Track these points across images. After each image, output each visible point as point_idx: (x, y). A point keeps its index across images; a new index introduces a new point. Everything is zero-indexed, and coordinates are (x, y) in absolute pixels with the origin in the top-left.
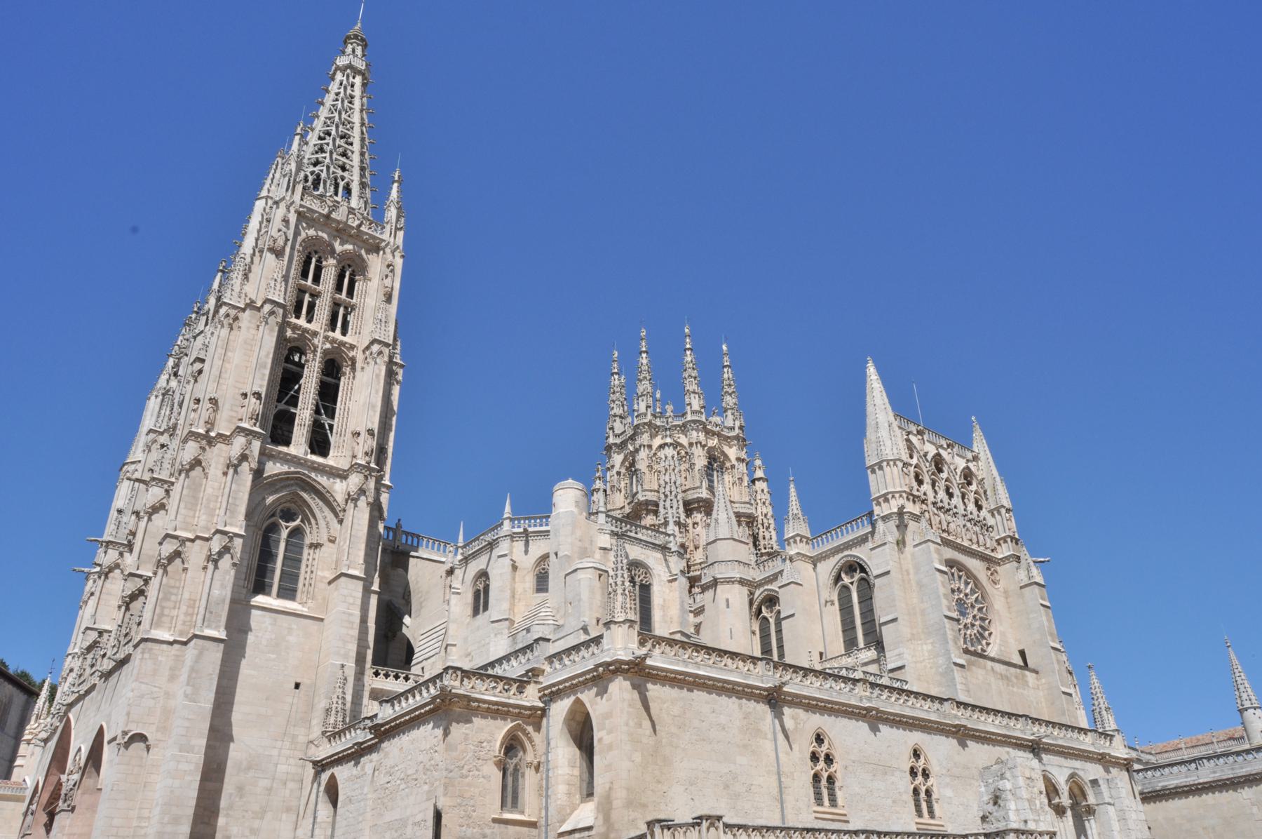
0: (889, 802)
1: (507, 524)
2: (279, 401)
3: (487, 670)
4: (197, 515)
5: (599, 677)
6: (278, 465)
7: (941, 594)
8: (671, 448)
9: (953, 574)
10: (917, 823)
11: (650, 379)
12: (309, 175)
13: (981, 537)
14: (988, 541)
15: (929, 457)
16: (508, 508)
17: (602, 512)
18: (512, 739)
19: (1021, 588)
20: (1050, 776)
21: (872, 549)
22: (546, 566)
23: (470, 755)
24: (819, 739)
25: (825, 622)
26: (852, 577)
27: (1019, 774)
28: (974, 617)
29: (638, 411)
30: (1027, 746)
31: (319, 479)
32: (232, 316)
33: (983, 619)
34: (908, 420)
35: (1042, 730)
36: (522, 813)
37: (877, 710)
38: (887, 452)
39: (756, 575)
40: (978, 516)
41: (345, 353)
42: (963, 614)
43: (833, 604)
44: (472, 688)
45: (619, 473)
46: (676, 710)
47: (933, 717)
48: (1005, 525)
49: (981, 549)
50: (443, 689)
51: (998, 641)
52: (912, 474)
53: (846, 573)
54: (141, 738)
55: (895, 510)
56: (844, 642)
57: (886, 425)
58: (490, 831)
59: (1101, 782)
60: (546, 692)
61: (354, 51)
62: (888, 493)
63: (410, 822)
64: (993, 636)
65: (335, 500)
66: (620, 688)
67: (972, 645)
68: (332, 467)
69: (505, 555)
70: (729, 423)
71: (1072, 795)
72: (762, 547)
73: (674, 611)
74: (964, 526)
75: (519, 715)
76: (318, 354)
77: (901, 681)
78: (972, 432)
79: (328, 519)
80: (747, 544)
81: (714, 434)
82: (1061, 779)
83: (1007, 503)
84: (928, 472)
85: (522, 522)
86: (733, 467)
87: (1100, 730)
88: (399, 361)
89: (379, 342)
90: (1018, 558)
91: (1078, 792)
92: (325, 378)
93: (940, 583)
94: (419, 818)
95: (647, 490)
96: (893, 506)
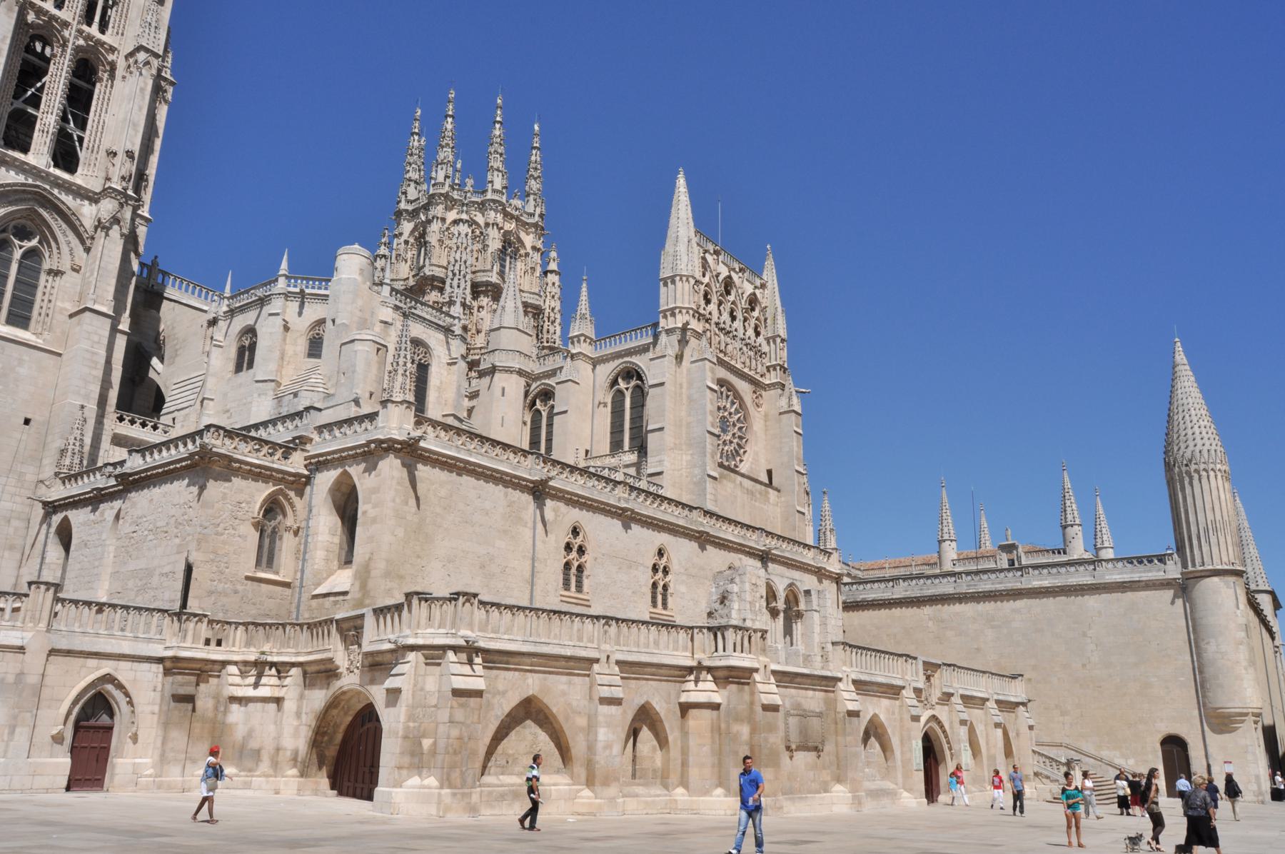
0: (629, 592)
1: (281, 284)
2: (16, 97)
3: (250, 431)
5: (370, 453)
6: (12, 173)
7: (708, 410)
8: (466, 225)
9: (722, 393)
10: (651, 613)
11: (453, 148)
13: (754, 362)
14: (759, 366)
15: (721, 278)
16: (284, 265)
17: (387, 284)
18: (272, 503)
19: (781, 414)
20: (772, 584)
21: (651, 360)
22: (321, 332)
23: (227, 514)
24: (575, 532)
25: (595, 422)
26: (628, 383)
27: (747, 580)
28: (734, 434)
29: (435, 179)
31: (63, 197)
33: (741, 438)
34: (707, 239)
35: (771, 543)
36: (277, 573)
37: (632, 511)
38: (682, 267)
39: (534, 367)
40: (755, 342)
41: (103, 55)
42: (724, 431)
43: (605, 405)
44: (235, 448)
45: (406, 242)
46: (443, 493)
47: (681, 522)
48: (779, 354)
49: (752, 373)
50: (203, 446)
51: (750, 459)
52: (702, 293)
53: (623, 379)
55: (680, 325)
56: (611, 443)
57: (686, 240)
58: (243, 587)
59: (813, 592)
60: (313, 461)
62: (676, 308)
63: (157, 572)
64: (746, 454)
65: (82, 225)
66: (391, 466)
67: (727, 460)
68: (80, 187)
69: (277, 314)
70: (530, 209)
71: (787, 601)
72: (544, 340)
73: (450, 395)
74: (741, 349)
75: (281, 481)
76: (69, 51)
77: (657, 485)
78: (764, 260)
79: (72, 245)
80: (531, 336)
81: (512, 217)
82: (781, 588)
83: (783, 333)
85: (299, 281)
86: (527, 255)
87: (822, 548)
88: (168, 76)
89: (147, 50)
90: (784, 386)
91: (792, 598)
93: (708, 400)
94: (166, 569)
96: (679, 321)
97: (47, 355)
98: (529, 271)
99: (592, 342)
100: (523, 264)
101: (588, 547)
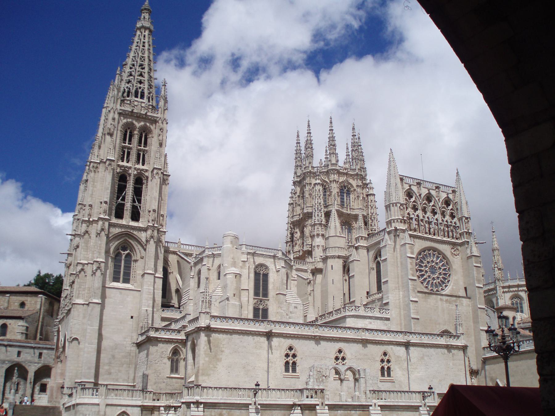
4: (88, 253)
6: (117, 229)
12: (126, 88)
20: (338, 369)
28: (440, 274)
30: (402, 344)
32: (95, 167)
36: (179, 374)
43: (373, 269)
45: (299, 196)
51: (452, 284)
54: (76, 339)
57: (394, 185)
61: (144, 17)
64: (450, 282)
65: (142, 241)
79: (140, 249)
84: (420, 204)
86: (355, 190)
89: (156, 169)
92: (137, 186)
95: (308, 207)
97: (135, 292)
98: (356, 198)
99: (366, 239)
100: (353, 195)
101: (297, 354)
